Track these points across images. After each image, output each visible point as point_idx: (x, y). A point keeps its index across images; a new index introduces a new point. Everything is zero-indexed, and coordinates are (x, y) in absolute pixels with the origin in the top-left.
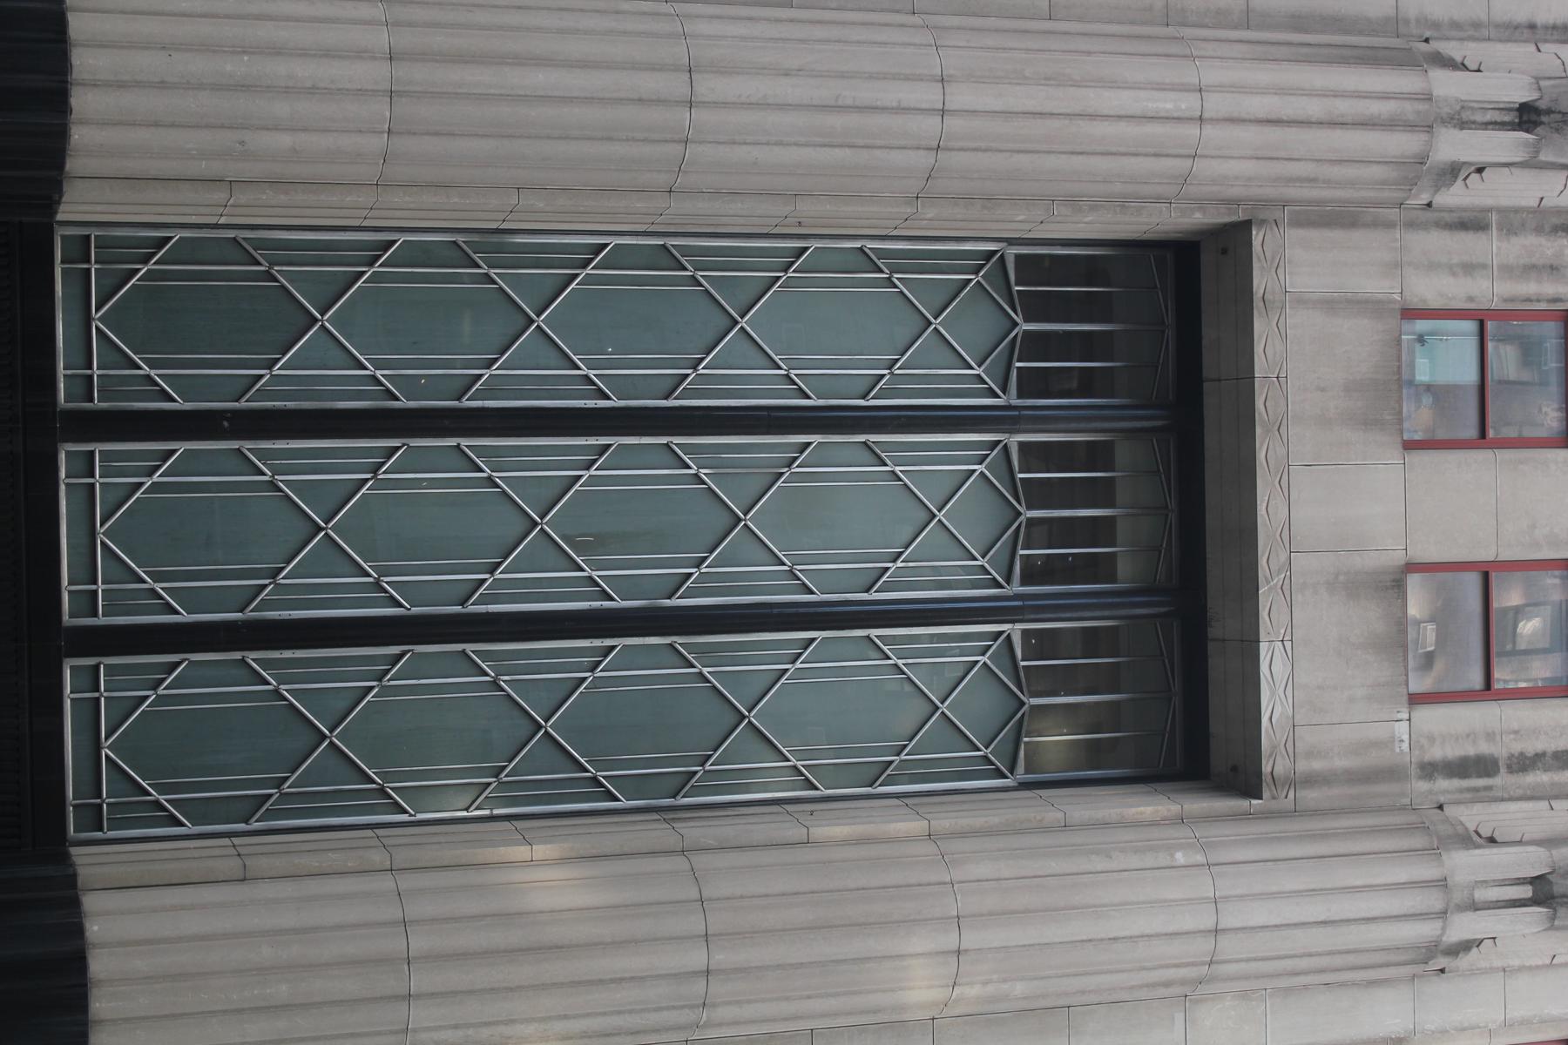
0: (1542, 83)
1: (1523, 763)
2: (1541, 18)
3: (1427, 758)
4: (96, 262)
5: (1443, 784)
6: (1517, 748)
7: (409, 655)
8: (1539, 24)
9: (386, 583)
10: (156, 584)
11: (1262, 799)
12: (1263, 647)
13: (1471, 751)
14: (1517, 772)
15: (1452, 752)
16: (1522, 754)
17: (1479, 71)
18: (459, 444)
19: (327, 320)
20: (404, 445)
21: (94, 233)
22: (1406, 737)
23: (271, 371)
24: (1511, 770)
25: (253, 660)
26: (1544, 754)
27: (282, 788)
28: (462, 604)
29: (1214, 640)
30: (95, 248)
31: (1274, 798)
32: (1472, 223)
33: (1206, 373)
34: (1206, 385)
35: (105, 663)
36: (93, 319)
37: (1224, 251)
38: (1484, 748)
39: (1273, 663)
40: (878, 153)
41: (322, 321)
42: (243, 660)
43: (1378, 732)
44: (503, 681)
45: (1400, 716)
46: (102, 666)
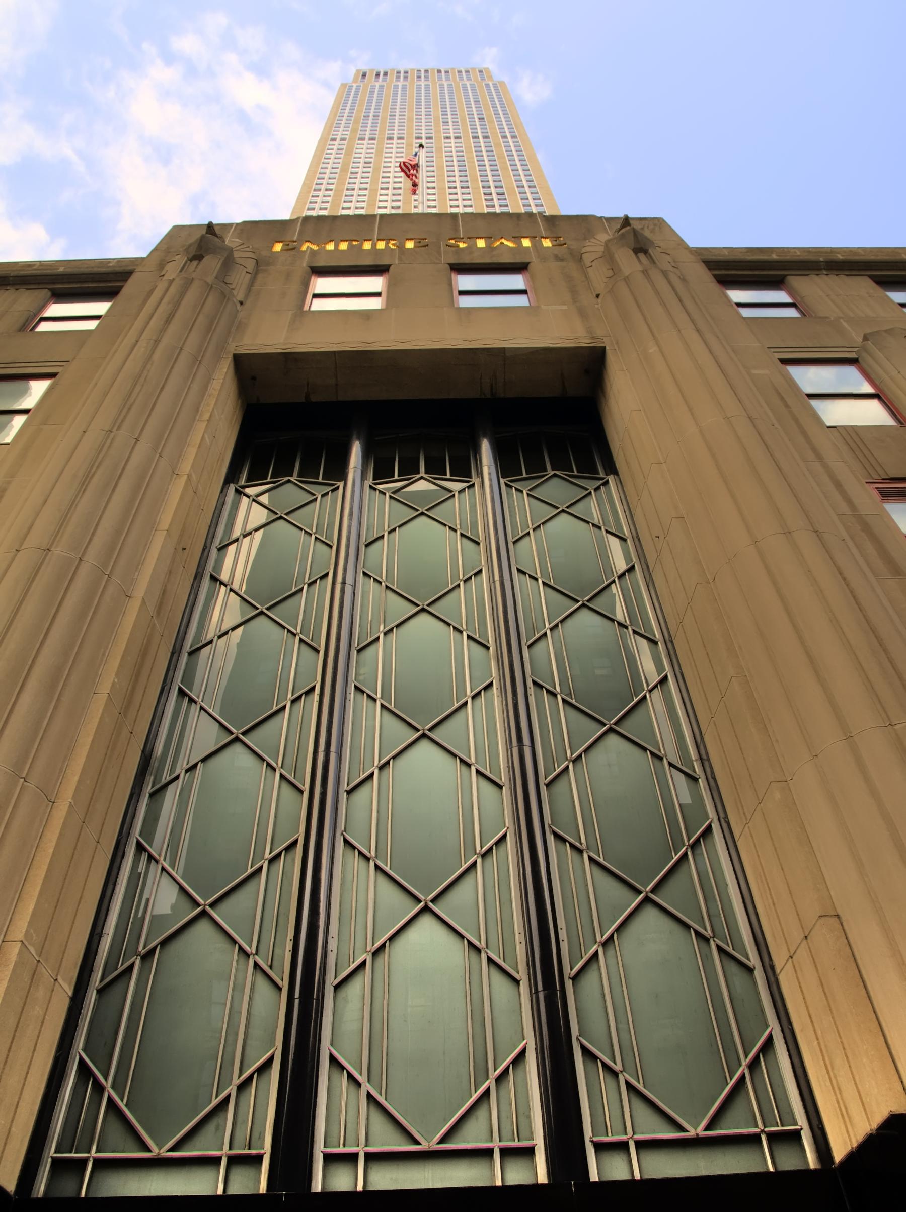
4: (89, 1151)
7: (553, 827)
9: (481, 848)
10: (491, 1076)
18: (346, 791)
19: (205, 901)
20: (342, 834)
21: (51, 1151)
23: (252, 954)
25: (571, 970)
27: (708, 937)
28: (500, 787)
30: (71, 1152)
34: (341, 398)
35: (591, 1134)
36: (159, 1154)
37: (254, 378)
40: (129, 467)
41: (205, 905)
42: (575, 979)
44: (572, 755)
46: (595, 1139)
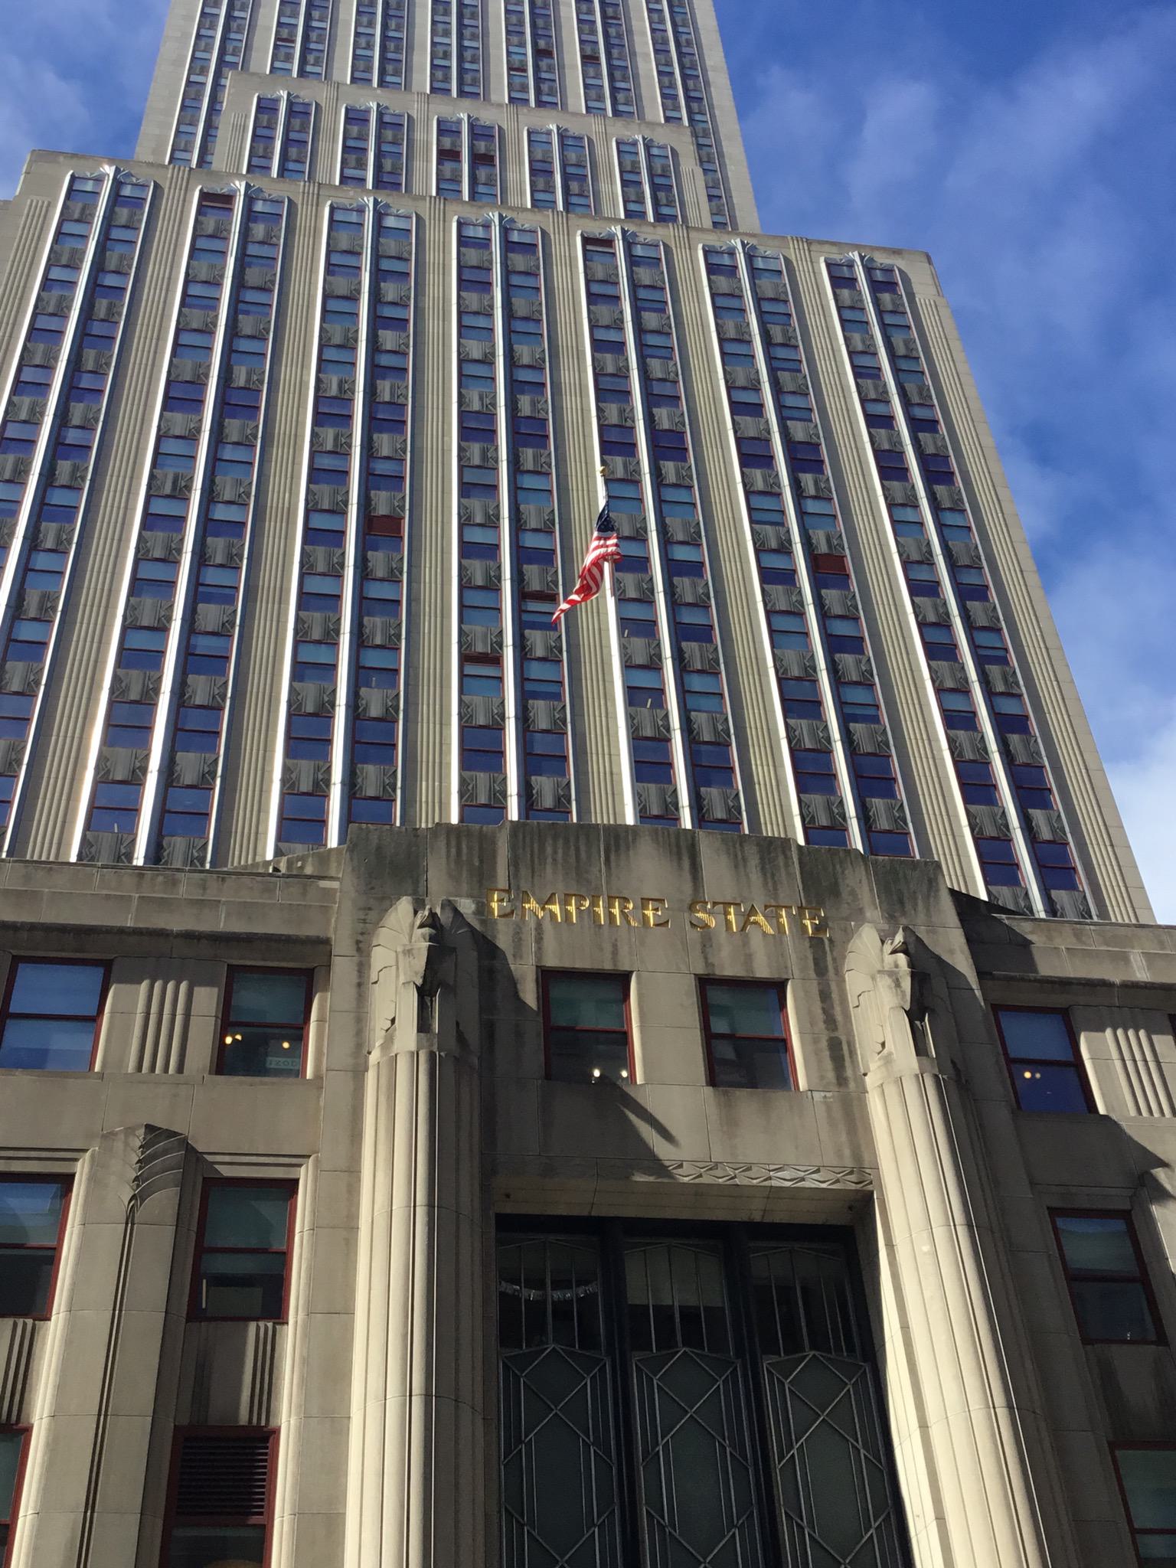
0: (402, 979)
1: (830, 1022)
2: (355, 980)
3: (834, 1081)
5: (849, 1073)
6: (822, 1026)
8: (357, 981)
11: (872, 1192)
12: (774, 1183)
13: (827, 1053)
14: (836, 1026)
15: (828, 1064)
16: (825, 1022)
17: (393, 1021)
22: (823, 1094)
24: (835, 1029)
26: (823, 1009)
29: (763, 1216)
31: (871, 1183)
32: (489, 1031)
33: (585, 1213)
38: (824, 1044)
39: (783, 1179)
43: (821, 1111)
45: (810, 1097)
